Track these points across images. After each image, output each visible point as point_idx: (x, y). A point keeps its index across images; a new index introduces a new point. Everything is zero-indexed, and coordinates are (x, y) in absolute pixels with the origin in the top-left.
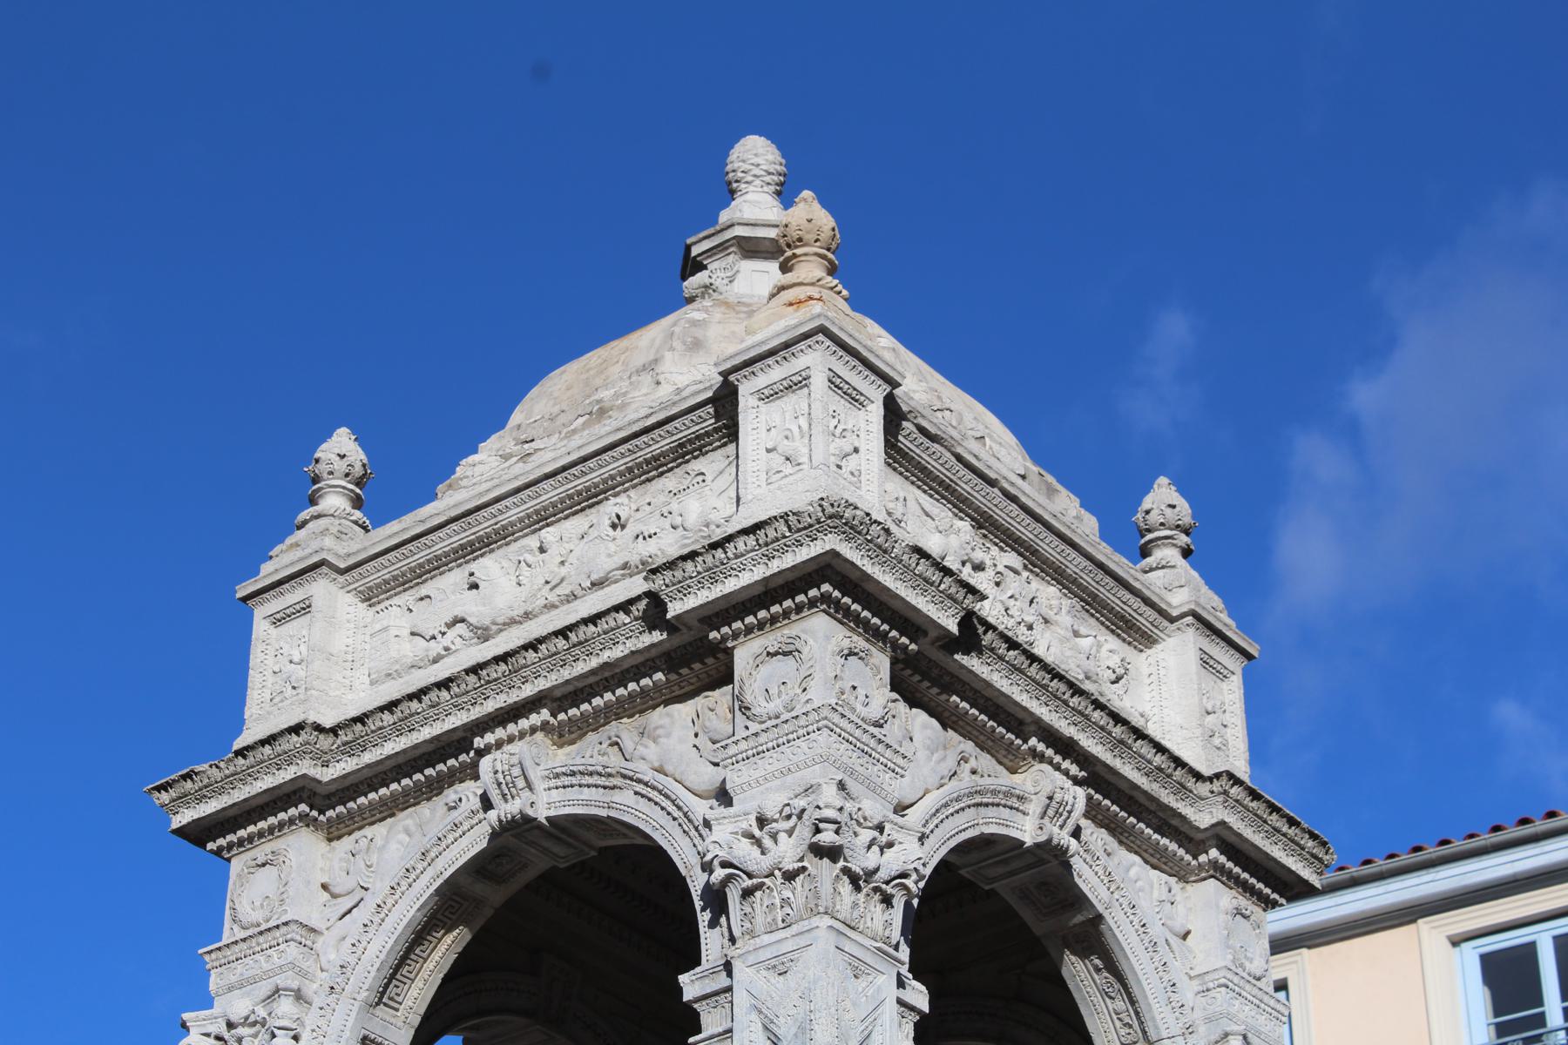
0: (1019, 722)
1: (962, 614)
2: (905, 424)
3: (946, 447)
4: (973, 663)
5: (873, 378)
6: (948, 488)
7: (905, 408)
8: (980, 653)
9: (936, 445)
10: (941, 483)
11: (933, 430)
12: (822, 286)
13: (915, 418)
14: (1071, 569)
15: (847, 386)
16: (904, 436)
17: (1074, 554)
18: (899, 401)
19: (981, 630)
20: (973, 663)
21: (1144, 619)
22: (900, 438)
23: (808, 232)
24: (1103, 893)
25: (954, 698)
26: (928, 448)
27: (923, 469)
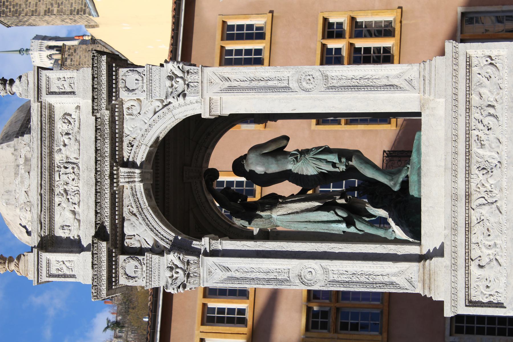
0: (113, 195)
1: (99, 241)
2: (43, 236)
3: (41, 217)
4: (107, 224)
5: (40, 259)
6: (50, 209)
7: (39, 239)
8: (103, 223)
9: (42, 221)
10: (50, 212)
11: (39, 225)
12: (19, 270)
13: (39, 233)
14: (47, 151)
15: (47, 268)
16: (46, 233)
17: (43, 152)
18: (39, 241)
19: (98, 226)
20: (107, 224)
21: (46, 113)
22: (47, 234)
23: (3, 270)
24: (143, 147)
25: (117, 222)
26: (44, 223)
27: (50, 221)
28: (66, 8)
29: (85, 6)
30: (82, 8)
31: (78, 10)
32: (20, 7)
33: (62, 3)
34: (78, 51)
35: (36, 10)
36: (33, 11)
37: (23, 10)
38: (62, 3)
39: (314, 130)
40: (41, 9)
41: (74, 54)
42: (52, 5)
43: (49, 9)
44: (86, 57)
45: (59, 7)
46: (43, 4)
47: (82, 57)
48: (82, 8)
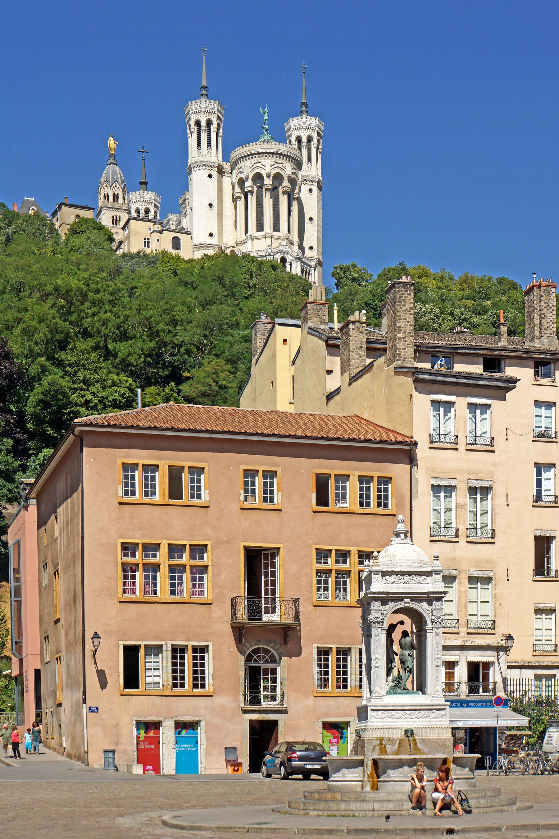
28: (401, 344)
29: (403, 360)
30: (401, 357)
31: (400, 354)
32: (403, 305)
33: (405, 341)
34: (361, 334)
35: (400, 319)
36: (400, 316)
37: (401, 308)
38: (405, 341)
39: (312, 547)
40: (401, 323)
41: (359, 331)
42: (404, 332)
43: (401, 330)
44: (356, 341)
45: (403, 338)
46: (405, 325)
47: (356, 339)
48: (401, 357)
